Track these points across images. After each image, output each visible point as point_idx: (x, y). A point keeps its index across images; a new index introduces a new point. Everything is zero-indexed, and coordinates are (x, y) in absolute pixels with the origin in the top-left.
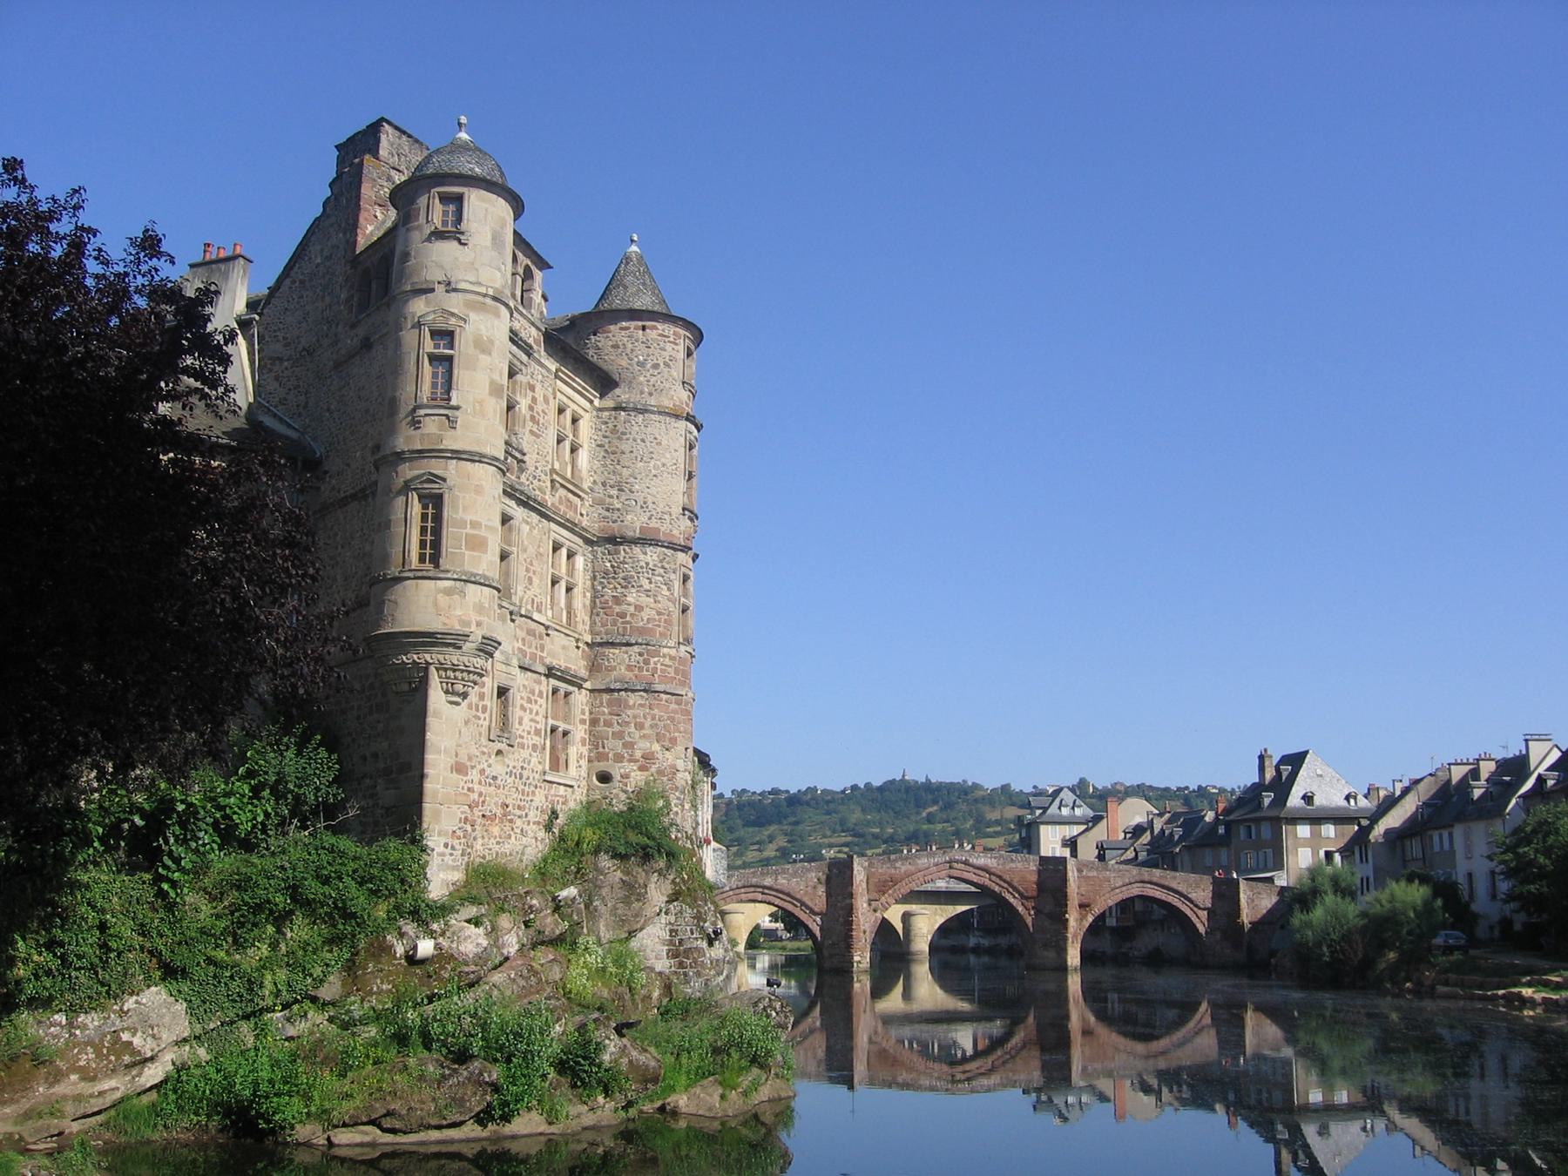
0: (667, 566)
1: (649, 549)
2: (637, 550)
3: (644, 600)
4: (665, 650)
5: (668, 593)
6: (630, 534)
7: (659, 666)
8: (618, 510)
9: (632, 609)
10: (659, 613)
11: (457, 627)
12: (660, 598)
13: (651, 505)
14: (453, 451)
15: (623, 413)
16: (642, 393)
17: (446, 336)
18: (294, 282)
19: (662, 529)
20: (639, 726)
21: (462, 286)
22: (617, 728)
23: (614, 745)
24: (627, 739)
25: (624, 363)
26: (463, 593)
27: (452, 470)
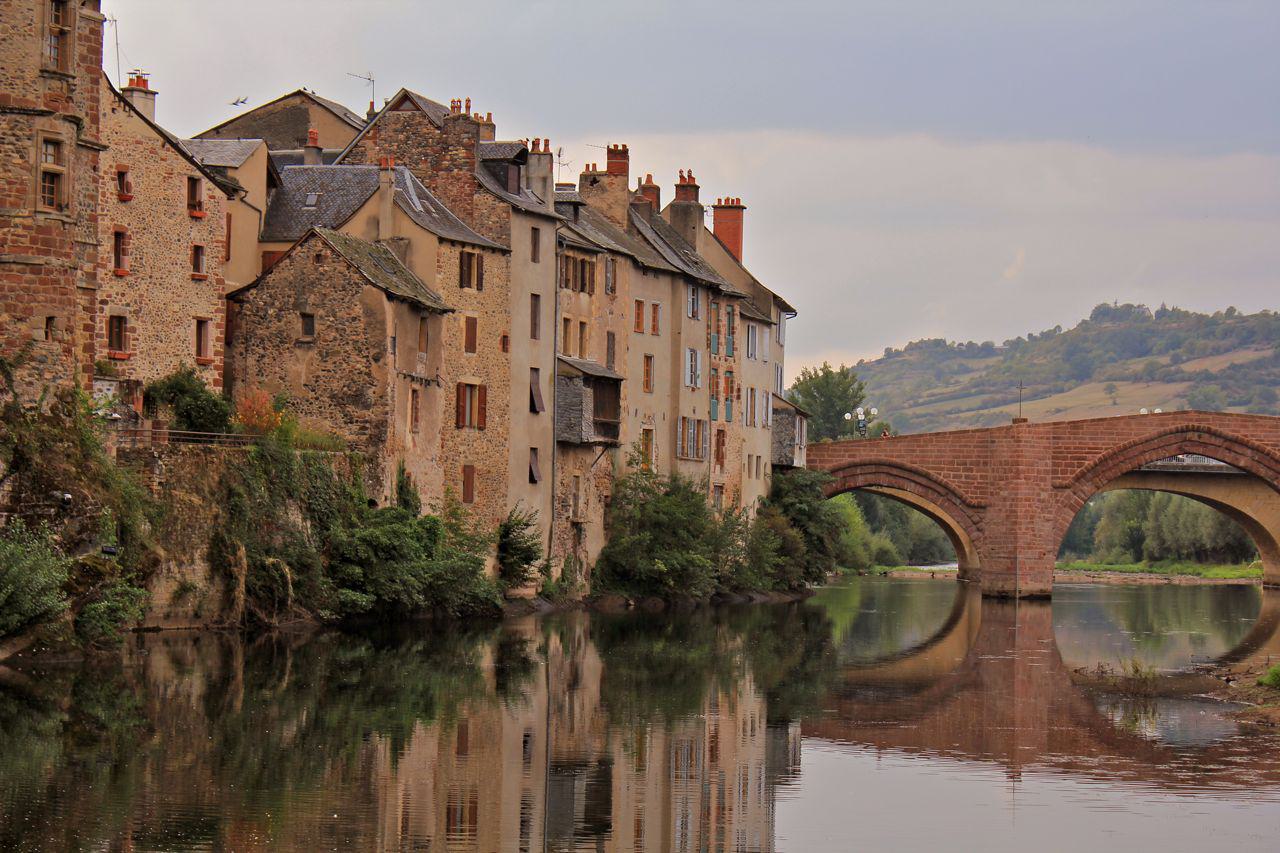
0: (19, 133)
4: (17, 220)
5: (20, 161)
7: (9, 237)
10: (10, 183)
19: (13, 95)
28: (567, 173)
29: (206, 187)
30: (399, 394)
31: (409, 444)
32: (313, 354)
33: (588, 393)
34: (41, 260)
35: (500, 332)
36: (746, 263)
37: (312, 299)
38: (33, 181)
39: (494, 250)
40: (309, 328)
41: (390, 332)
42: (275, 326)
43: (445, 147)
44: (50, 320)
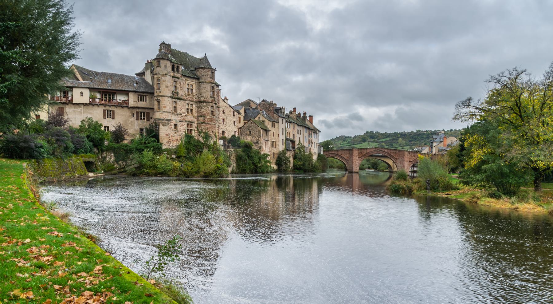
2: (203, 103)
3: (204, 110)
11: (163, 118)
17: (158, 80)
27: (160, 98)
28: (287, 112)
29: (235, 113)
30: (263, 142)
31: (265, 149)
32: (251, 136)
33: (291, 143)
34: (211, 123)
35: (278, 133)
36: (314, 124)
37: (251, 129)
38: (209, 112)
39: (277, 122)
40: (250, 133)
41: (262, 134)
42: (245, 132)
43: (270, 107)
44: (212, 131)
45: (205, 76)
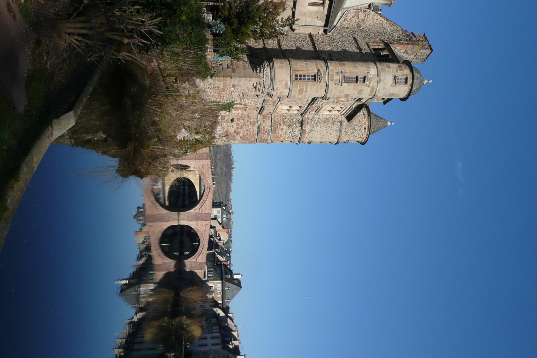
0: (294, 137)
1: (299, 132)
2: (299, 128)
3: (284, 131)
4: (270, 137)
5: (286, 137)
6: (304, 126)
8: (311, 123)
9: (281, 127)
10: (280, 135)
11: (275, 87)
12: (285, 135)
13: (313, 132)
14: (328, 85)
15: (340, 124)
16: (346, 129)
18: (382, 21)
19: (305, 135)
20: (247, 130)
21: (379, 85)
22: (247, 124)
23: (241, 122)
24: (244, 127)
25: (355, 124)
26: (286, 88)
45: (354, 133)
